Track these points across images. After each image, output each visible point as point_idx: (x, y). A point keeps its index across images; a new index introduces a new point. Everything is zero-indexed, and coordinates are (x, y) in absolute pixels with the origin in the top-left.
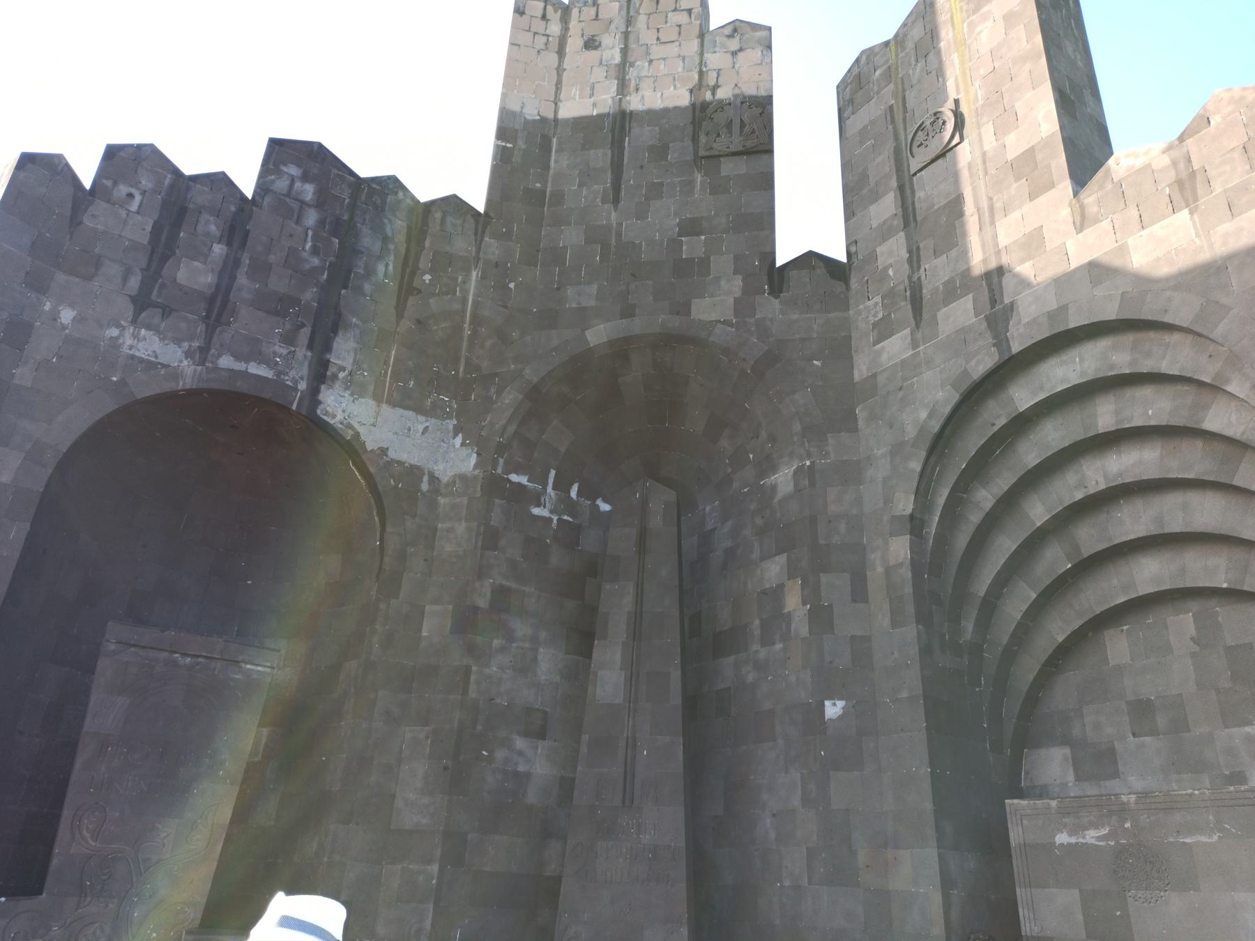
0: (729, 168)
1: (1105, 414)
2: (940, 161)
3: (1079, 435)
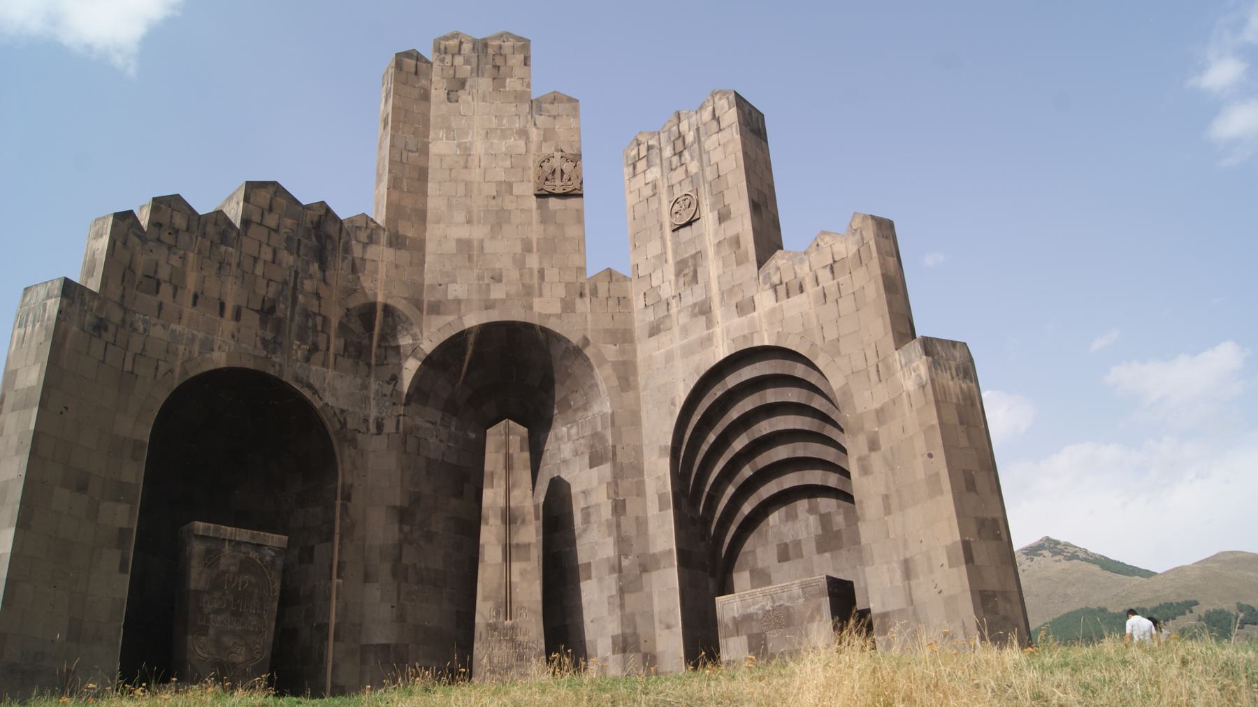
0: (552, 202)
1: (772, 396)
2: (688, 228)
3: (759, 404)
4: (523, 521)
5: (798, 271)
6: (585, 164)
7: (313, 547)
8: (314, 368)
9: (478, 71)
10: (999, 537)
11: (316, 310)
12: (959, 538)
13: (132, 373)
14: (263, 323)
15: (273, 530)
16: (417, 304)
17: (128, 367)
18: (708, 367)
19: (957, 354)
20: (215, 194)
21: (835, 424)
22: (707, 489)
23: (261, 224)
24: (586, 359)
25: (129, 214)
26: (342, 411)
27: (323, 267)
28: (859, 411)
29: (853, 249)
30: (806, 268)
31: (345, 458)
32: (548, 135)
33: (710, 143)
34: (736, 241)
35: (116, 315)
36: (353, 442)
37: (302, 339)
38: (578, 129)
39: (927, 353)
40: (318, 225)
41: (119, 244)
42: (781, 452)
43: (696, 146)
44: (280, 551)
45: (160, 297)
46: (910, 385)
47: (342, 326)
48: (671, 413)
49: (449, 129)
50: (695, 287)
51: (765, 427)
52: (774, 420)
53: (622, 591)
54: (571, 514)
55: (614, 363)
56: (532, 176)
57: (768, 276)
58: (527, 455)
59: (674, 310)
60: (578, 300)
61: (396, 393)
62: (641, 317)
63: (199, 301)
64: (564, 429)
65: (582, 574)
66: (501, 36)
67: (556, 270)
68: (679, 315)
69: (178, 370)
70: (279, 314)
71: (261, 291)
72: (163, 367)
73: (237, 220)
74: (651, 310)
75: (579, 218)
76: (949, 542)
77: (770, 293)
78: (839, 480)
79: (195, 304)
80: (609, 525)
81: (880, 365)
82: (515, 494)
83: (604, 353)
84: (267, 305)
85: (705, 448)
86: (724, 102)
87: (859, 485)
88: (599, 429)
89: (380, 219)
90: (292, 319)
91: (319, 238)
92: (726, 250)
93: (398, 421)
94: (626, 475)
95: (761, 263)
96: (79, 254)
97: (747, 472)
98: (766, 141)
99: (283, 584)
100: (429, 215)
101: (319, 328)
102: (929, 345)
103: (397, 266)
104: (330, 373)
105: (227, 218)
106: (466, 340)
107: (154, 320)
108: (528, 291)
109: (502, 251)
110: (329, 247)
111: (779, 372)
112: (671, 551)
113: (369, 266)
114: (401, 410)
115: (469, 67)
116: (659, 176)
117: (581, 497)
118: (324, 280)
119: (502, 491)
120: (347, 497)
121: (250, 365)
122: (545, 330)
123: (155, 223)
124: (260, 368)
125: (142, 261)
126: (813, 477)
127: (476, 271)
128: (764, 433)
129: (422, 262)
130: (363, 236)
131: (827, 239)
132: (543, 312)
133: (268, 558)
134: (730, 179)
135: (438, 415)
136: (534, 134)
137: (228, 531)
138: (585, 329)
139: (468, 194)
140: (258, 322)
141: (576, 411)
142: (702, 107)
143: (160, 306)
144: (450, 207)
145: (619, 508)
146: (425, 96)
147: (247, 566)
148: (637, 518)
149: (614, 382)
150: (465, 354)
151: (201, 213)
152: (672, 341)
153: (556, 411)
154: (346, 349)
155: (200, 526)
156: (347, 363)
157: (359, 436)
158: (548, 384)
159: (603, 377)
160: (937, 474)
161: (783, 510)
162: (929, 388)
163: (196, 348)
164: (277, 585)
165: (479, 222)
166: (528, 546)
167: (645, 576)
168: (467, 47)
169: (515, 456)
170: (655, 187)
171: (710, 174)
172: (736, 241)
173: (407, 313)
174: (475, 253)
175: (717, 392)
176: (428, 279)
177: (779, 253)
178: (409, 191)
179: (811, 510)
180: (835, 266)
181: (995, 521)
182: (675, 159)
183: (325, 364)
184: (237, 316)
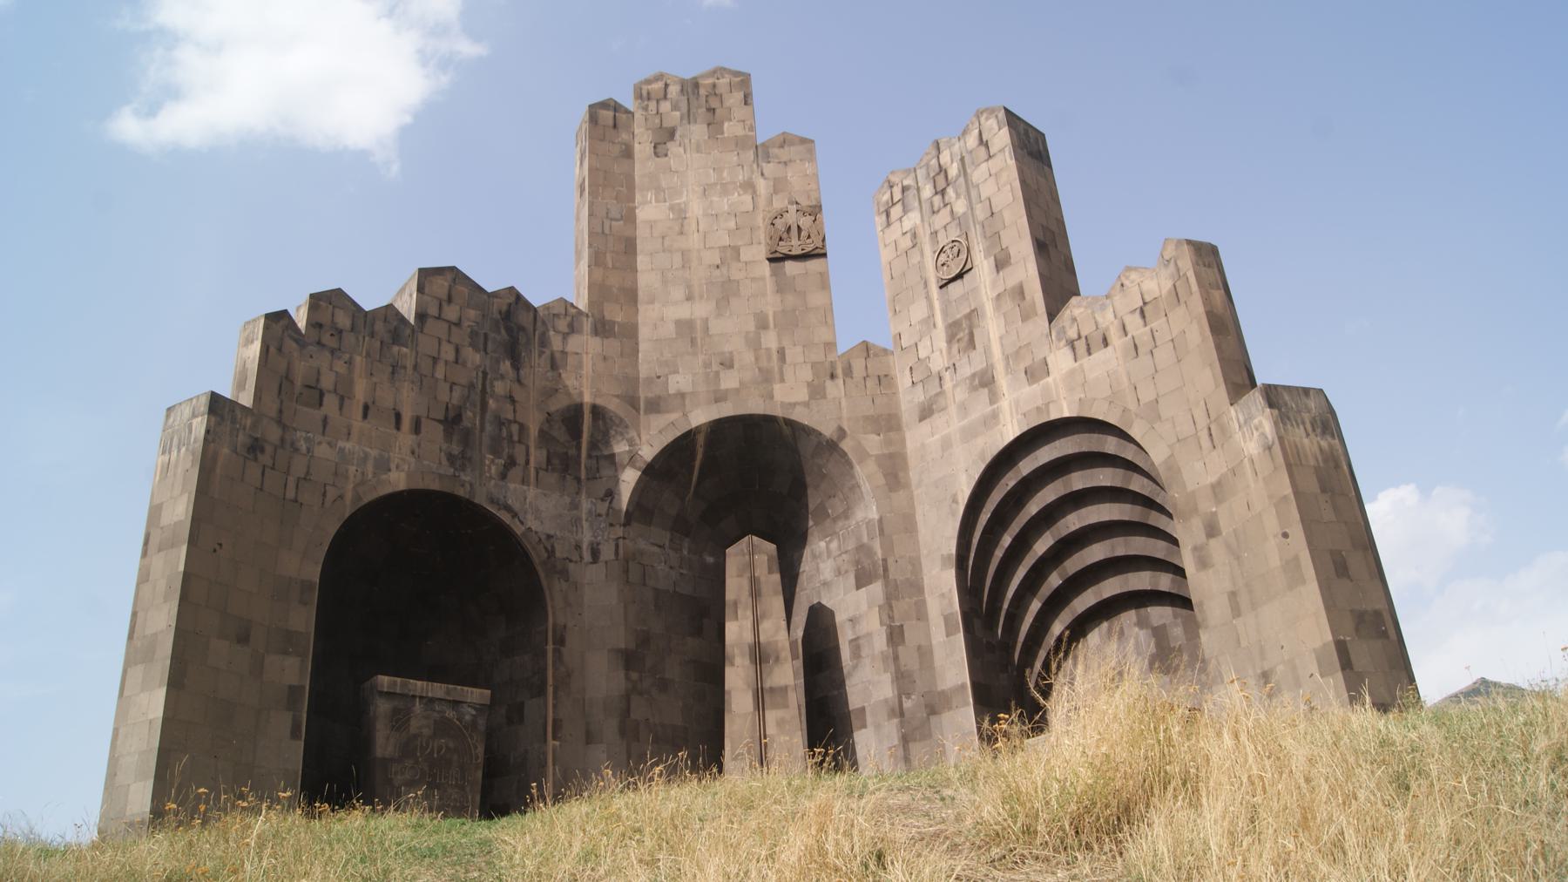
0: (790, 266)
1: (1079, 480)
2: (959, 282)
4: (777, 659)
5: (1099, 319)
6: (827, 217)
7: (522, 704)
8: (512, 486)
9: (689, 117)
10: (1385, 635)
11: (510, 416)
12: (1330, 638)
13: (296, 501)
14: (448, 435)
15: (474, 684)
16: (633, 402)
17: (291, 494)
18: (995, 452)
19: (1312, 404)
20: (382, 285)
21: (1161, 509)
22: (1006, 606)
23: (439, 318)
24: (844, 454)
25: (284, 314)
26: (549, 537)
27: (516, 366)
28: (1190, 488)
29: (1167, 285)
30: (1110, 316)
31: (555, 592)
32: (778, 186)
33: (978, 175)
34: (1020, 292)
35: (274, 433)
36: (564, 574)
37: (496, 452)
38: (816, 175)
39: (1271, 405)
40: (507, 316)
41: (272, 349)
42: (1096, 552)
43: (962, 179)
44: (481, 709)
45: (324, 410)
46: (1252, 447)
47: (544, 436)
48: (954, 514)
49: (658, 189)
50: (973, 354)
51: (1073, 522)
52: (1083, 511)
53: (905, 740)
54: (837, 648)
55: (878, 457)
56: (762, 237)
57: (1063, 331)
58: (776, 577)
59: (948, 385)
60: (829, 383)
61: (612, 510)
62: (908, 398)
63: (370, 413)
64: (823, 544)
65: (855, 722)
66: (714, 72)
67: (799, 349)
68: (956, 392)
69: (349, 496)
70: (466, 423)
71: (444, 396)
72: (332, 493)
74: (919, 387)
75: (824, 283)
76: (1318, 644)
77: (1067, 351)
78: (1173, 581)
79: (365, 416)
80: (885, 658)
81: (1213, 428)
82: (766, 626)
83: (865, 446)
84: (451, 414)
85: (999, 553)
86: (992, 123)
87: (1200, 584)
88: (865, 540)
89: (582, 304)
90: (482, 429)
91: (509, 330)
92: (1008, 304)
93: (617, 546)
94: (902, 594)
95: (1051, 316)
96: (228, 364)
97: (1054, 580)
98: (1050, 166)
99: (488, 750)
100: (640, 293)
101: (516, 438)
102: (1273, 396)
103: (605, 358)
104: (532, 492)
105: (398, 313)
107: (319, 438)
108: (766, 377)
109: (730, 331)
110: (522, 340)
111: (1084, 449)
112: (963, 686)
113: (570, 359)
114: (619, 531)
115: (678, 114)
116: (918, 221)
117: (848, 625)
118: (519, 381)
119: (748, 624)
120: (560, 641)
122: (790, 423)
123: (311, 323)
125: (301, 370)
126: (1140, 581)
127: (701, 358)
128: (1073, 528)
130: (562, 325)
131: (1134, 276)
132: (787, 400)
133: (468, 717)
134: (1007, 215)
135: (665, 537)
136: (762, 186)
137: (418, 686)
138: (840, 418)
139: (685, 265)
140: (441, 434)
141: (835, 520)
142: (965, 132)
143: (325, 420)
144: (665, 282)
145: (895, 636)
146: (628, 153)
147: (442, 727)
148: (919, 648)
149: (881, 481)
150: (694, 459)
151: (367, 307)
152: (949, 423)
153: (811, 523)
154: (549, 461)
155: (384, 681)
156: (551, 478)
157: (571, 566)
158: (798, 489)
159: (866, 475)
160: (1296, 558)
161: (1105, 625)
162: (1277, 448)
163: (370, 468)
164: (480, 750)
165: (701, 297)
166: (784, 689)
167: (933, 719)
168: (674, 90)
169: (763, 579)
170: (915, 235)
171: (981, 213)
172: (1020, 292)
173: (621, 414)
174: (699, 335)
175: (1009, 481)
176: (644, 370)
177: (1074, 300)
178: (614, 267)
179: (1142, 623)
180: (1146, 309)
181: (1377, 614)
182: (937, 200)
183: (524, 481)
184: (417, 427)
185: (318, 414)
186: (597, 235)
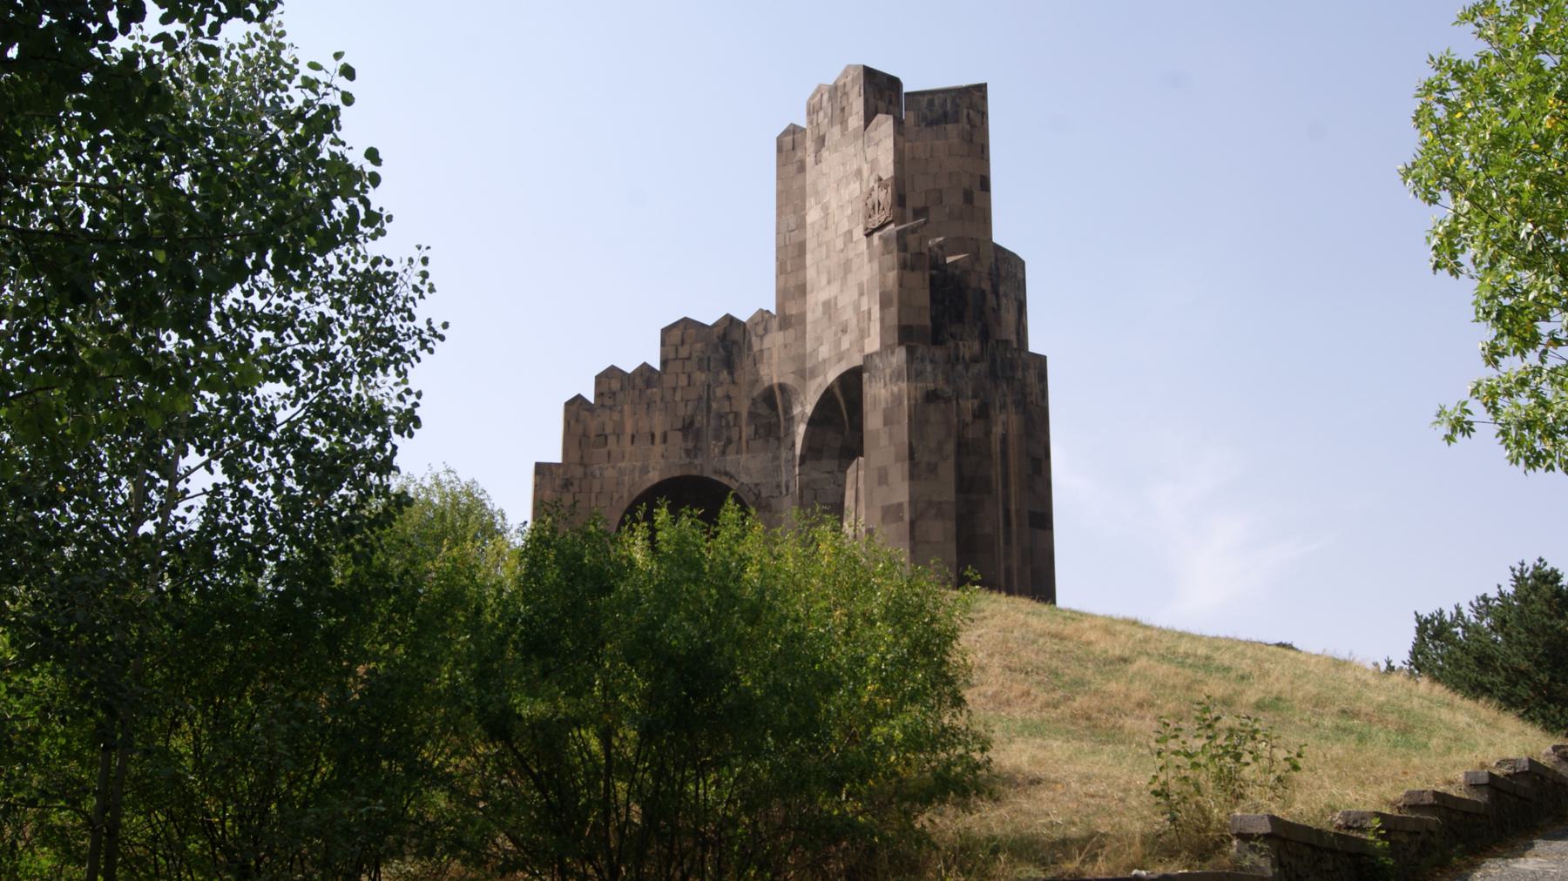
8: (729, 458)
10: (901, 519)
14: (685, 437)
20: (640, 350)
25: (579, 397)
27: (731, 373)
35: (578, 472)
37: (717, 438)
40: (724, 337)
69: (626, 495)
70: (697, 425)
71: (681, 411)
72: (616, 496)
73: (657, 366)
91: (725, 348)
104: (743, 458)
106: (834, 394)
113: (766, 355)
118: (733, 382)
121: (677, 473)
123: (599, 395)
124: (685, 472)
125: (593, 427)
129: (804, 332)
130: (760, 330)
151: (629, 370)
157: (773, 501)
163: (637, 474)
184: (665, 439)
185: (605, 451)
186: (781, 249)
